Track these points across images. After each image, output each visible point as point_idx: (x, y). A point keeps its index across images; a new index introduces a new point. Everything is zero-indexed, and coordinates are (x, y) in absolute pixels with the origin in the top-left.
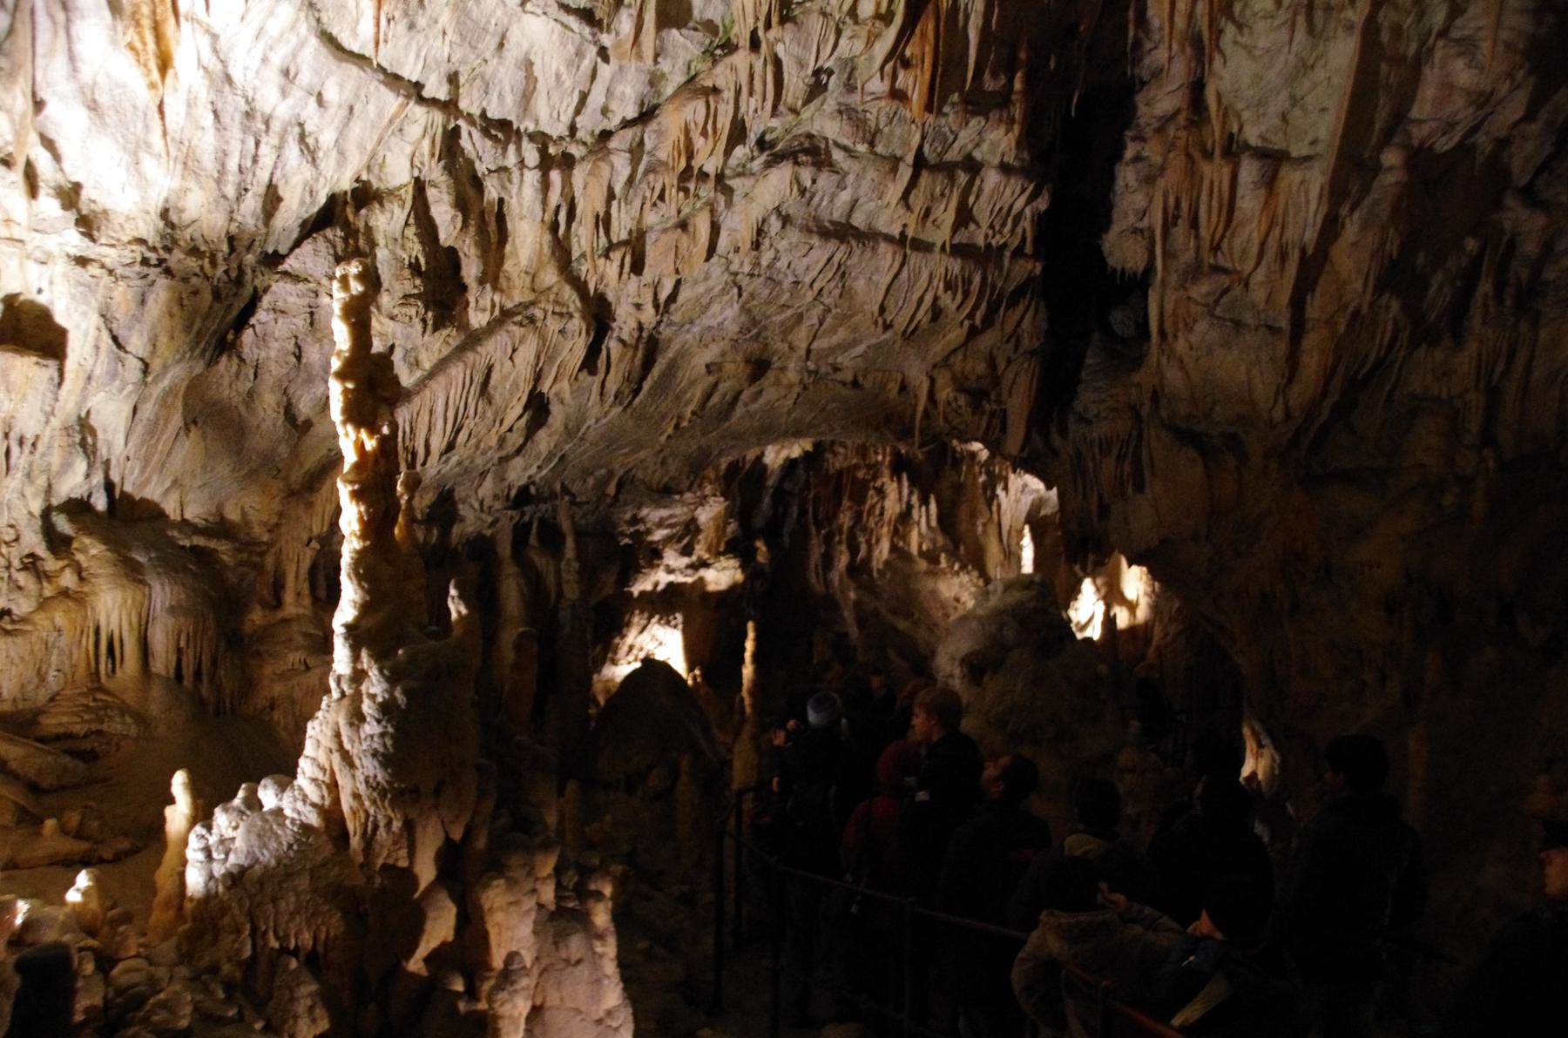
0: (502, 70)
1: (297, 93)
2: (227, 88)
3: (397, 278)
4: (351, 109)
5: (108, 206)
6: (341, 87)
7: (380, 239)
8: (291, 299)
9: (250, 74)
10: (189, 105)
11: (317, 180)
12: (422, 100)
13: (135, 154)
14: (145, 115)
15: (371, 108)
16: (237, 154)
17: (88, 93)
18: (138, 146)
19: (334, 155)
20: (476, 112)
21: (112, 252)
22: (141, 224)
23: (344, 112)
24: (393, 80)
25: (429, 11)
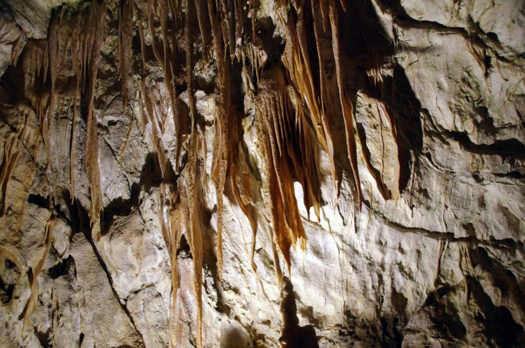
0: (489, 215)
1: (389, 251)
2: (356, 255)
3: (470, 324)
4: (418, 252)
5: (326, 314)
6: (408, 243)
7: (459, 309)
8: (415, 342)
9: (364, 247)
10: (341, 265)
11: (418, 287)
12: (454, 240)
13: (325, 289)
14: (325, 274)
15: (428, 248)
16: (371, 282)
17: (302, 270)
18: (325, 286)
19: (420, 273)
20: (486, 238)
21: (329, 332)
22: (337, 318)
23: (414, 254)
24: (434, 235)
25: (434, 200)
